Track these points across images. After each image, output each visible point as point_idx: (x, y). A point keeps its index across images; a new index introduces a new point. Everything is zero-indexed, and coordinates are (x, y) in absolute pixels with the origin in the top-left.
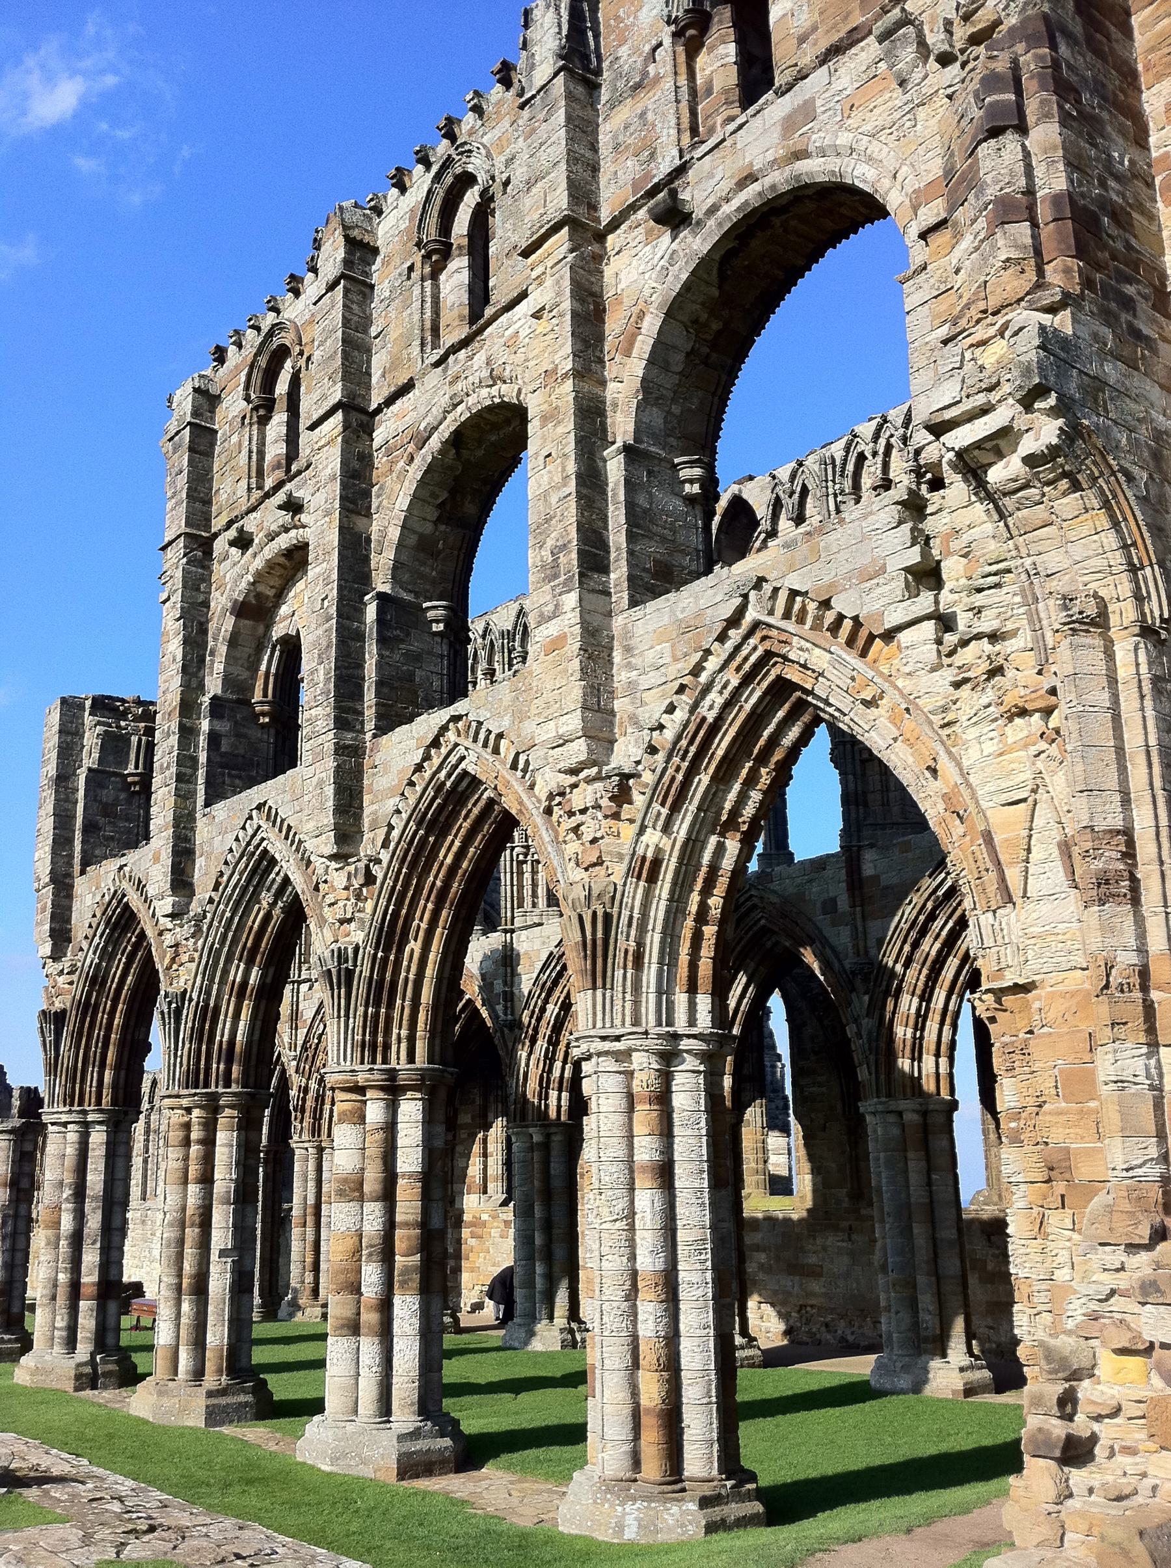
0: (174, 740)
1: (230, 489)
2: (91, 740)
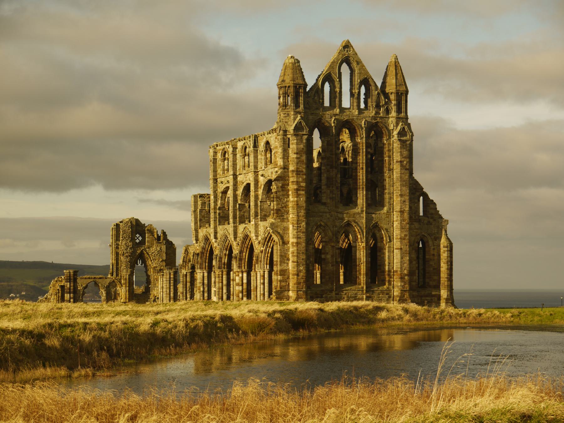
0: (213, 214)
1: (220, 171)
2: (199, 203)
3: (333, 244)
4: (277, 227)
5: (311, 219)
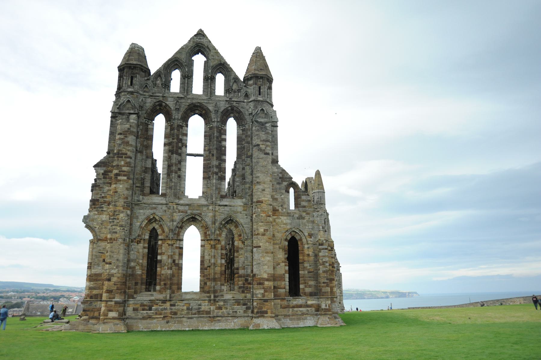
3: (170, 242)
4: (93, 220)
5: (141, 211)
